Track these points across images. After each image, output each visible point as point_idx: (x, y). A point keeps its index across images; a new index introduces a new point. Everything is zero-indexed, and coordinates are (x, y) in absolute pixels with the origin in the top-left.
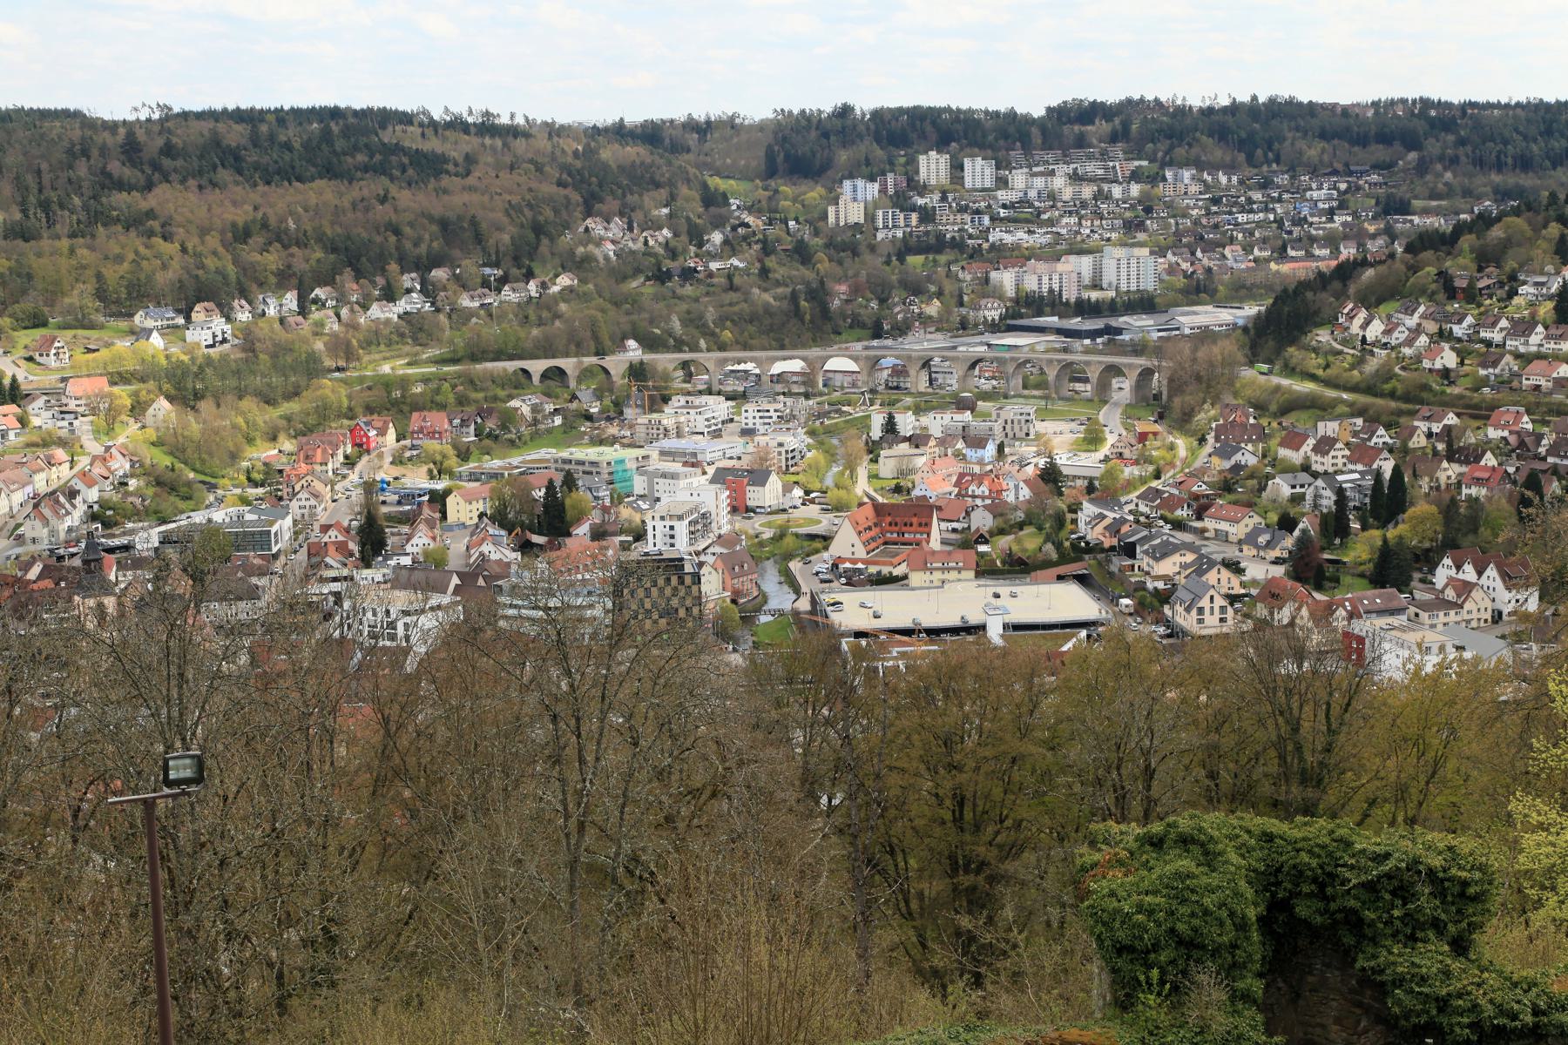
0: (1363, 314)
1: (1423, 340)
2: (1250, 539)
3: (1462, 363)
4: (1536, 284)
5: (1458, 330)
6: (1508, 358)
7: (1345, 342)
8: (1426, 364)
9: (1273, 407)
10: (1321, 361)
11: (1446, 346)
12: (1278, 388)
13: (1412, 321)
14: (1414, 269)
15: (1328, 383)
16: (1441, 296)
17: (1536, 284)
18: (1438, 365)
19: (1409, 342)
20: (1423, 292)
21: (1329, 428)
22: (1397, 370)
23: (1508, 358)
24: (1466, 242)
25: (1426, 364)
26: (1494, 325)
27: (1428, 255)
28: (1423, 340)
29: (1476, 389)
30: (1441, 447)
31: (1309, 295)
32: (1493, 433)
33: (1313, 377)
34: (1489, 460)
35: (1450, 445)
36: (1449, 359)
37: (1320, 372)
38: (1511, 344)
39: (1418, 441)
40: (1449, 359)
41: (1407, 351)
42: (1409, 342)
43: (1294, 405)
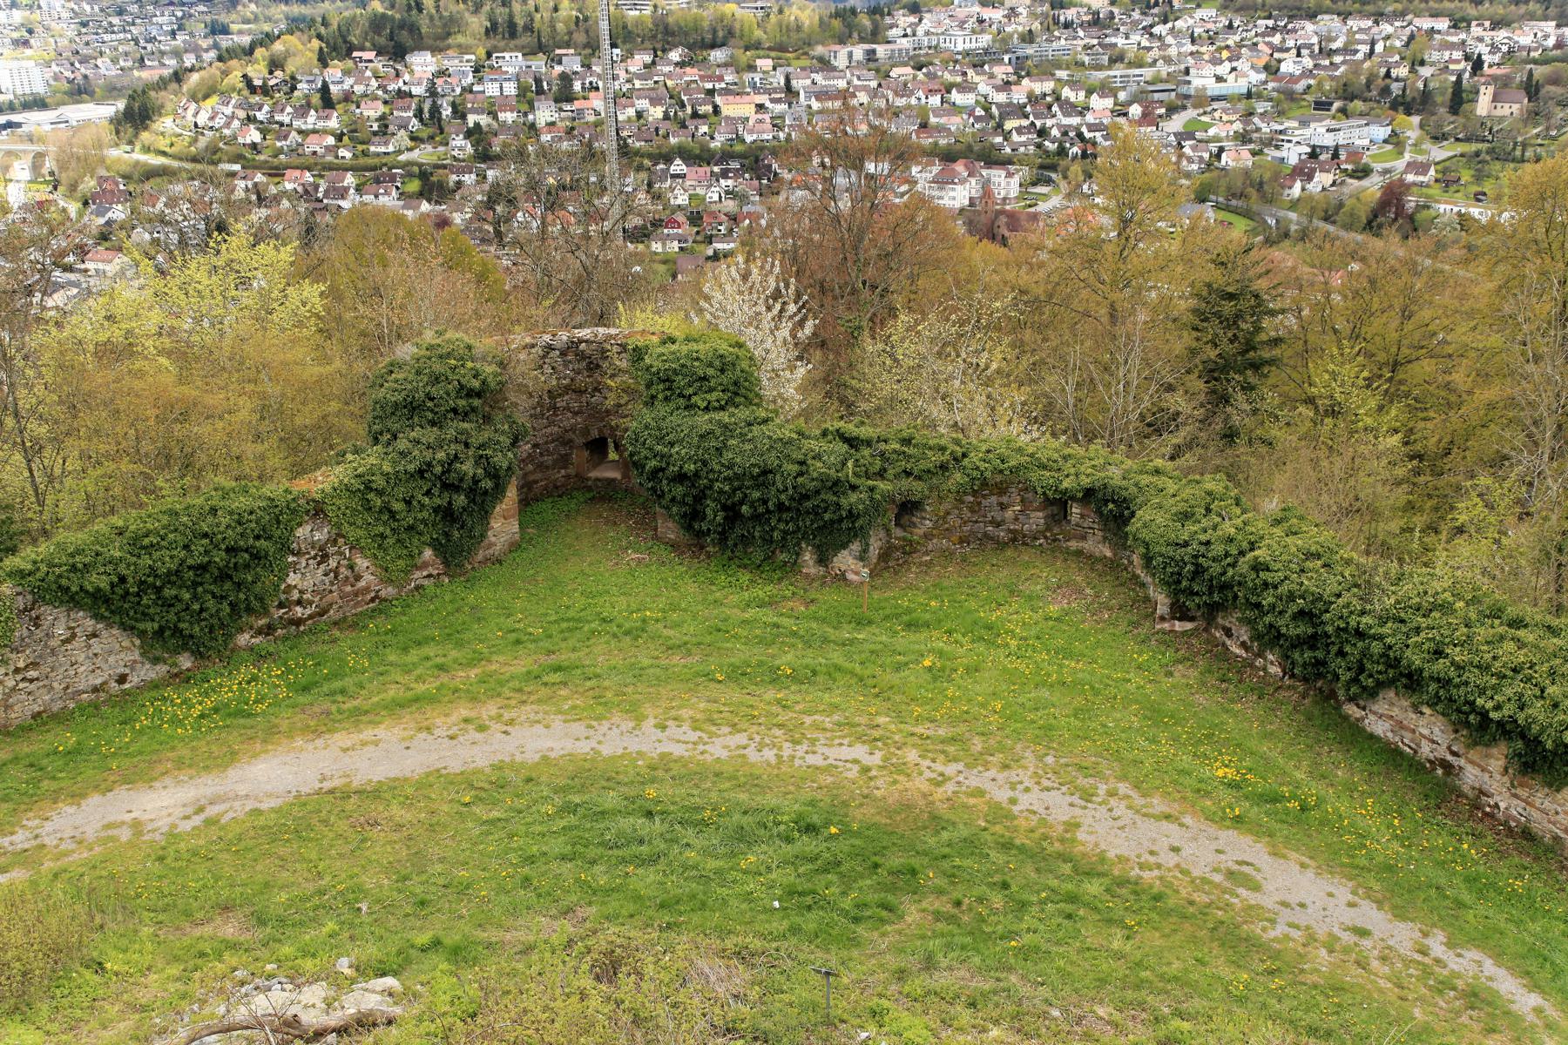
0: (193, 106)
1: (236, 123)
2: (122, 273)
3: (265, 138)
4: (308, 82)
5: (260, 116)
6: (294, 134)
7: (184, 128)
8: (241, 140)
9: (136, 176)
10: (168, 142)
11: (252, 126)
12: (137, 163)
13: (228, 110)
14: (226, 73)
15: (174, 157)
16: (246, 92)
17: (308, 82)
18: (248, 141)
19: (228, 125)
20: (234, 89)
21: (178, 188)
22: (221, 145)
23: (294, 134)
24: (260, 53)
25: (241, 140)
26: (282, 111)
27: (234, 63)
28: (236, 123)
29: (276, 156)
30: (254, 197)
31: (153, 94)
32: (289, 186)
33: (164, 154)
34: (285, 204)
35: (259, 198)
36: (254, 136)
37: (167, 150)
38: (297, 124)
39: (239, 194)
40: (254, 136)
41: (226, 132)
42: (228, 125)
43: (151, 174)
